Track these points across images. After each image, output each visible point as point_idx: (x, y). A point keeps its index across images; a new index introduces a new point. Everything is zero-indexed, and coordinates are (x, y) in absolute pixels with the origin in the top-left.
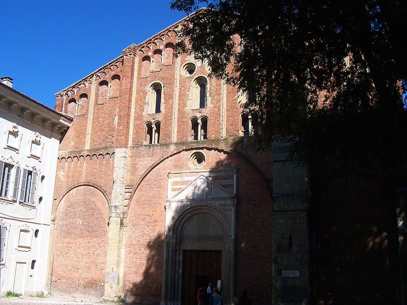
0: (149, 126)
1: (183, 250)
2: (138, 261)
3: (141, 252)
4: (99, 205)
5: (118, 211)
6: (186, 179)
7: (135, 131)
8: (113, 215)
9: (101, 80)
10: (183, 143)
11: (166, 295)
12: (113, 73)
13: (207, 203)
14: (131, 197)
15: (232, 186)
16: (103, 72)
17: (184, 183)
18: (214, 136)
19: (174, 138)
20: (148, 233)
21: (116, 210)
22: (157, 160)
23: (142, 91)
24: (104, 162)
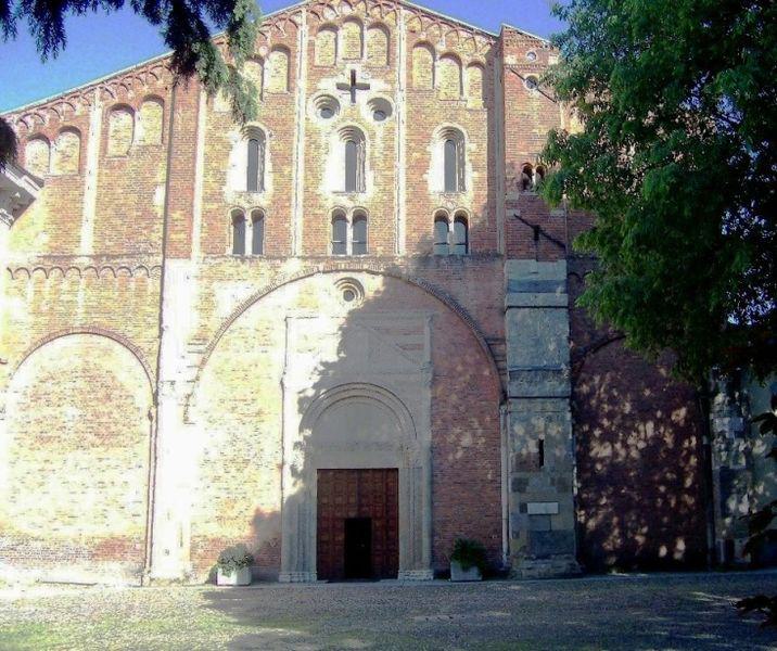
0: (238, 219)
3: (229, 476)
4: (122, 377)
9: (116, 100)
10: (318, 259)
12: (146, 90)
14: (204, 362)
16: (122, 84)
18: (382, 248)
19: (297, 246)
23: (220, 139)
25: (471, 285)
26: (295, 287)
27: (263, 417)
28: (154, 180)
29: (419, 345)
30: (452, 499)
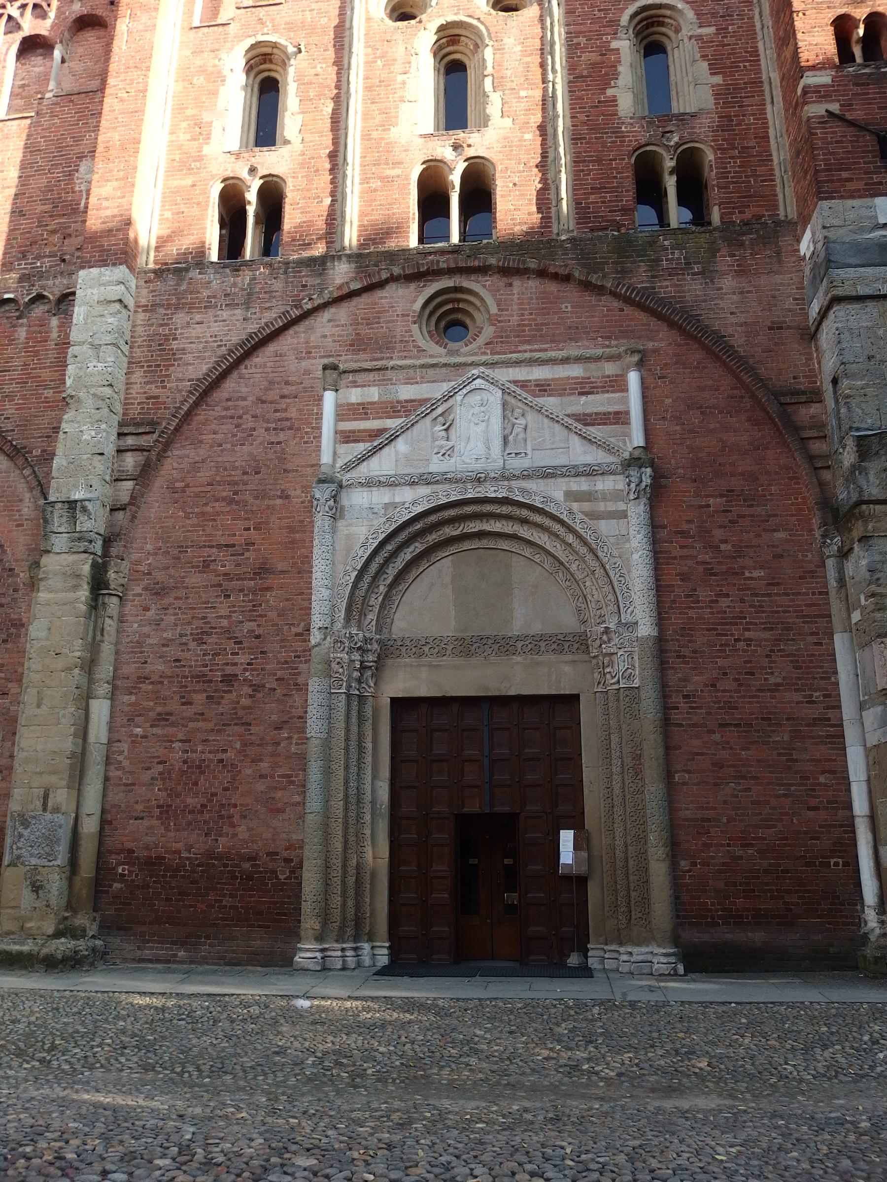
1: (393, 700)
2: (177, 754)
3: (189, 711)
5: (85, 524)
6: (406, 392)
7: (168, 215)
8: (60, 542)
11: (325, 916)
13: (510, 489)
15: (620, 418)
17: (394, 409)
20: (225, 623)
21: (73, 519)
22: (271, 316)
24: (22, 333)
25: (728, 283)
26: (342, 313)
27: (272, 581)
28: (76, 150)
29: (617, 413)
30: (719, 765)
